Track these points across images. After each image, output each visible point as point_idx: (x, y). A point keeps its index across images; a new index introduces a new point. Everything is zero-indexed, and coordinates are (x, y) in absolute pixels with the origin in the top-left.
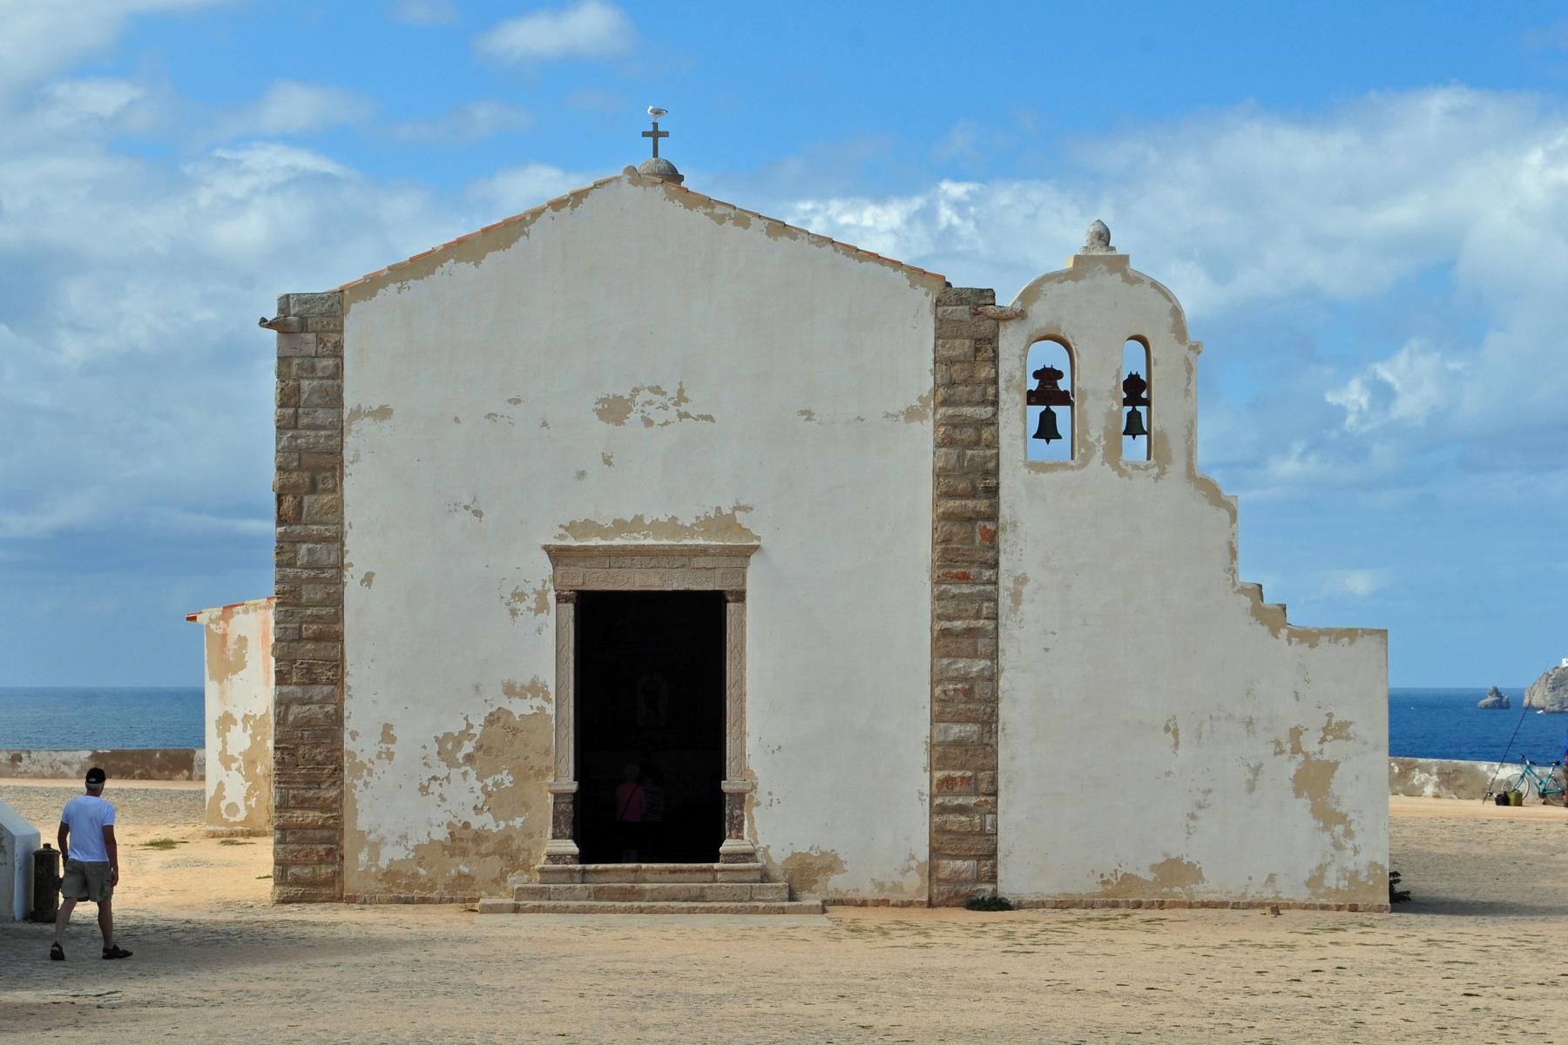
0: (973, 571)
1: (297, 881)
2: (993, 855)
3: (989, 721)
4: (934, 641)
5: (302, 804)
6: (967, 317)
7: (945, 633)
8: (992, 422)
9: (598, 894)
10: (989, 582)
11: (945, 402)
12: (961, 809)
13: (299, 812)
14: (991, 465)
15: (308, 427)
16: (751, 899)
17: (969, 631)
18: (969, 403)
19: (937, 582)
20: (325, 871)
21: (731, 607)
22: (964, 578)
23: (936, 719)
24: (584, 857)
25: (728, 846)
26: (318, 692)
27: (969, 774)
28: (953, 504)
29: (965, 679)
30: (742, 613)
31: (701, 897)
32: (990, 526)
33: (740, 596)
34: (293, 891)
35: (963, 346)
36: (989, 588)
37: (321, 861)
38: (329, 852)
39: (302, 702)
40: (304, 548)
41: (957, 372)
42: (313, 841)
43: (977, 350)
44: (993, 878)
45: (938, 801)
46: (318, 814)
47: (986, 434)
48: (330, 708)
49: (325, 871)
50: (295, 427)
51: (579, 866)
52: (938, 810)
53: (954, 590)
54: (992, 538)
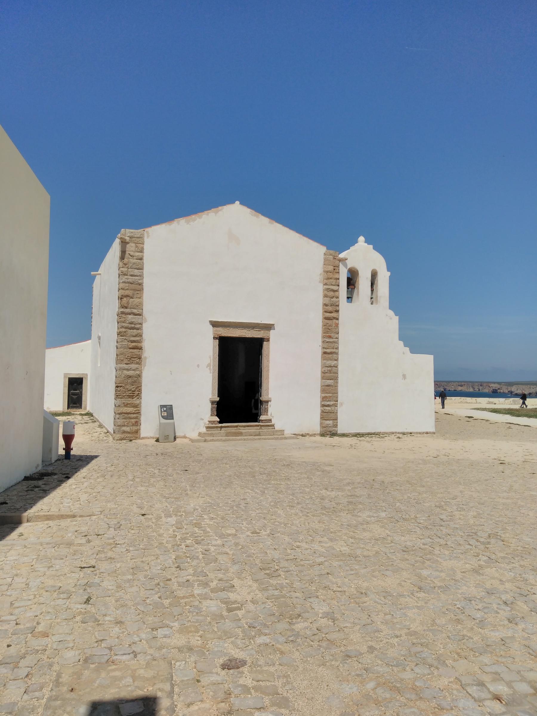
0: (332, 335)
1: (124, 432)
2: (337, 419)
3: (336, 379)
4: (322, 355)
5: (126, 405)
6: (332, 259)
7: (325, 353)
8: (337, 291)
9: (227, 435)
10: (336, 338)
11: (326, 284)
12: (328, 406)
13: (126, 408)
14: (337, 304)
15: (132, 276)
16: (274, 435)
17: (331, 353)
18: (332, 285)
19: (323, 337)
20: (135, 428)
21: (265, 343)
22: (330, 337)
23: (323, 378)
24: (220, 422)
25: (262, 418)
26: (133, 366)
27: (331, 395)
28: (328, 315)
29: (330, 367)
30: (269, 345)
31: (259, 435)
32: (337, 321)
33: (268, 340)
34: (123, 436)
35: (331, 268)
36: (336, 340)
37: (133, 425)
38: (136, 422)
39: (128, 370)
40: (130, 317)
41: (331, 275)
42: (131, 418)
43: (334, 269)
44: (336, 426)
45: (323, 403)
46: (132, 409)
47: (337, 293)
48: (138, 372)
49: (135, 428)
50: (127, 275)
51: (220, 425)
52: (323, 406)
53: (328, 340)
54: (337, 325)
